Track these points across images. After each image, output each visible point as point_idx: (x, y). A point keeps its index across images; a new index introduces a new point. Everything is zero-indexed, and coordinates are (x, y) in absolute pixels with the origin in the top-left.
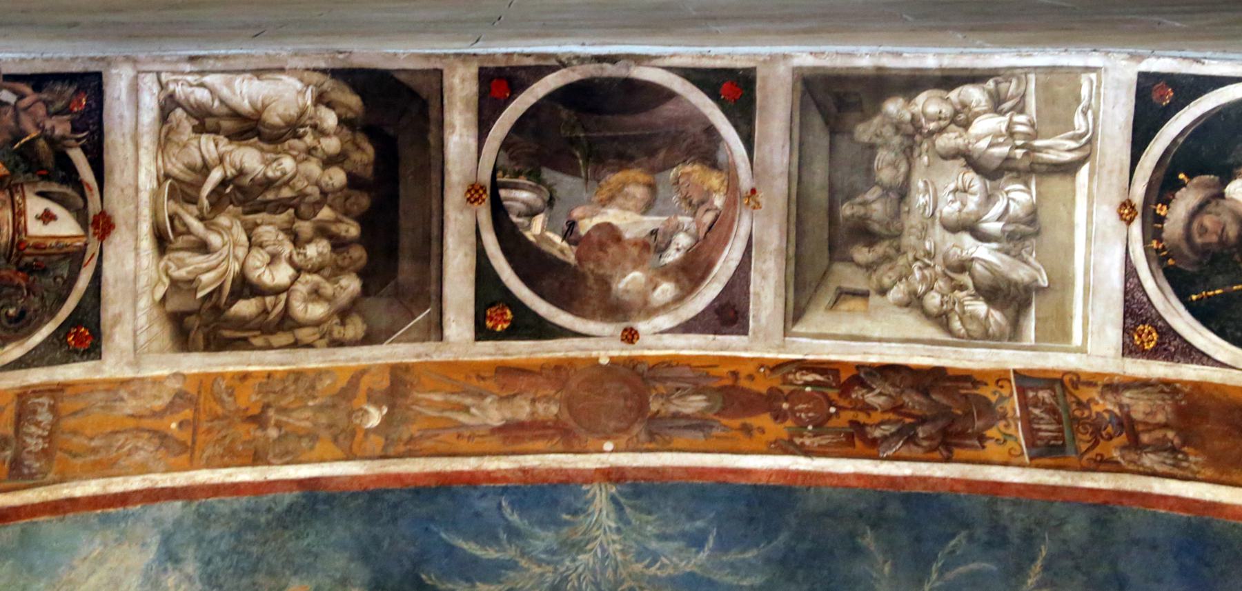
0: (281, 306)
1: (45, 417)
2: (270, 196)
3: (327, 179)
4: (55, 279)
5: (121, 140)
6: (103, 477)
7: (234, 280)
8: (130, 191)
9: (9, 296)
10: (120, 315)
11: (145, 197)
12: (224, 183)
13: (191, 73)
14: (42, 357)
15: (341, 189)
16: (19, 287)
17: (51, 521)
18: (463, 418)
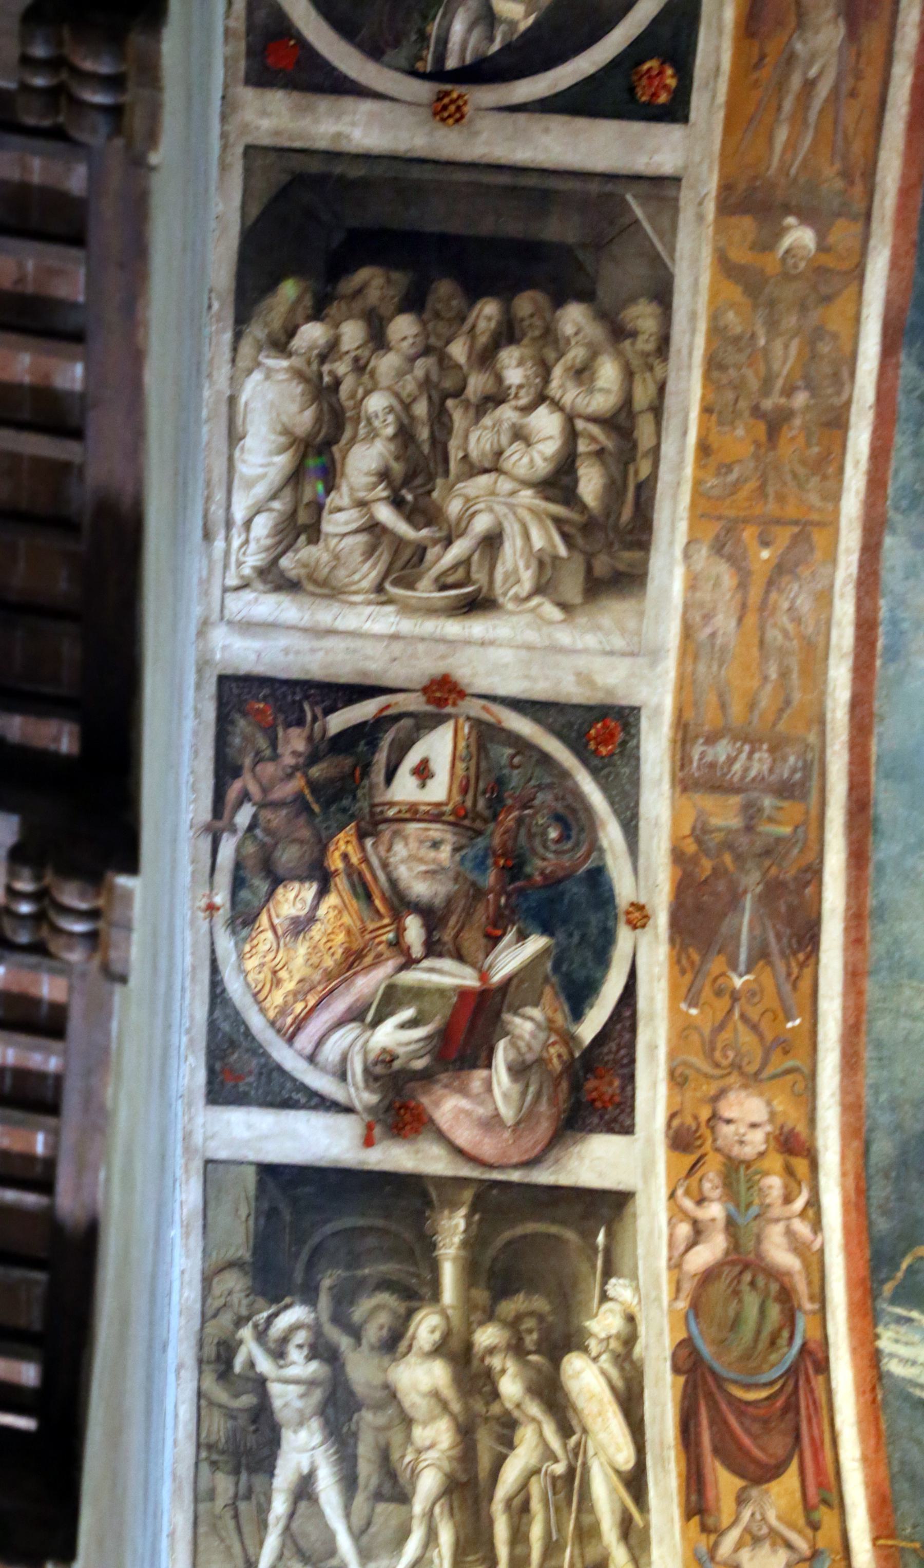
0: (595, 430)
1: (722, 750)
2: (424, 434)
3: (405, 344)
4: (514, 767)
5: (320, 655)
6: (826, 657)
7: (547, 499)
8: (397, 648)
9: (531, 836)
10: (578, 674)
11: (407, 626)
12: (397, 503)
13: (228, 539)
14: (625, 795)
15: (424, 324)
16: (520, 821)
17: (880, 735)
18: (823, 90)
